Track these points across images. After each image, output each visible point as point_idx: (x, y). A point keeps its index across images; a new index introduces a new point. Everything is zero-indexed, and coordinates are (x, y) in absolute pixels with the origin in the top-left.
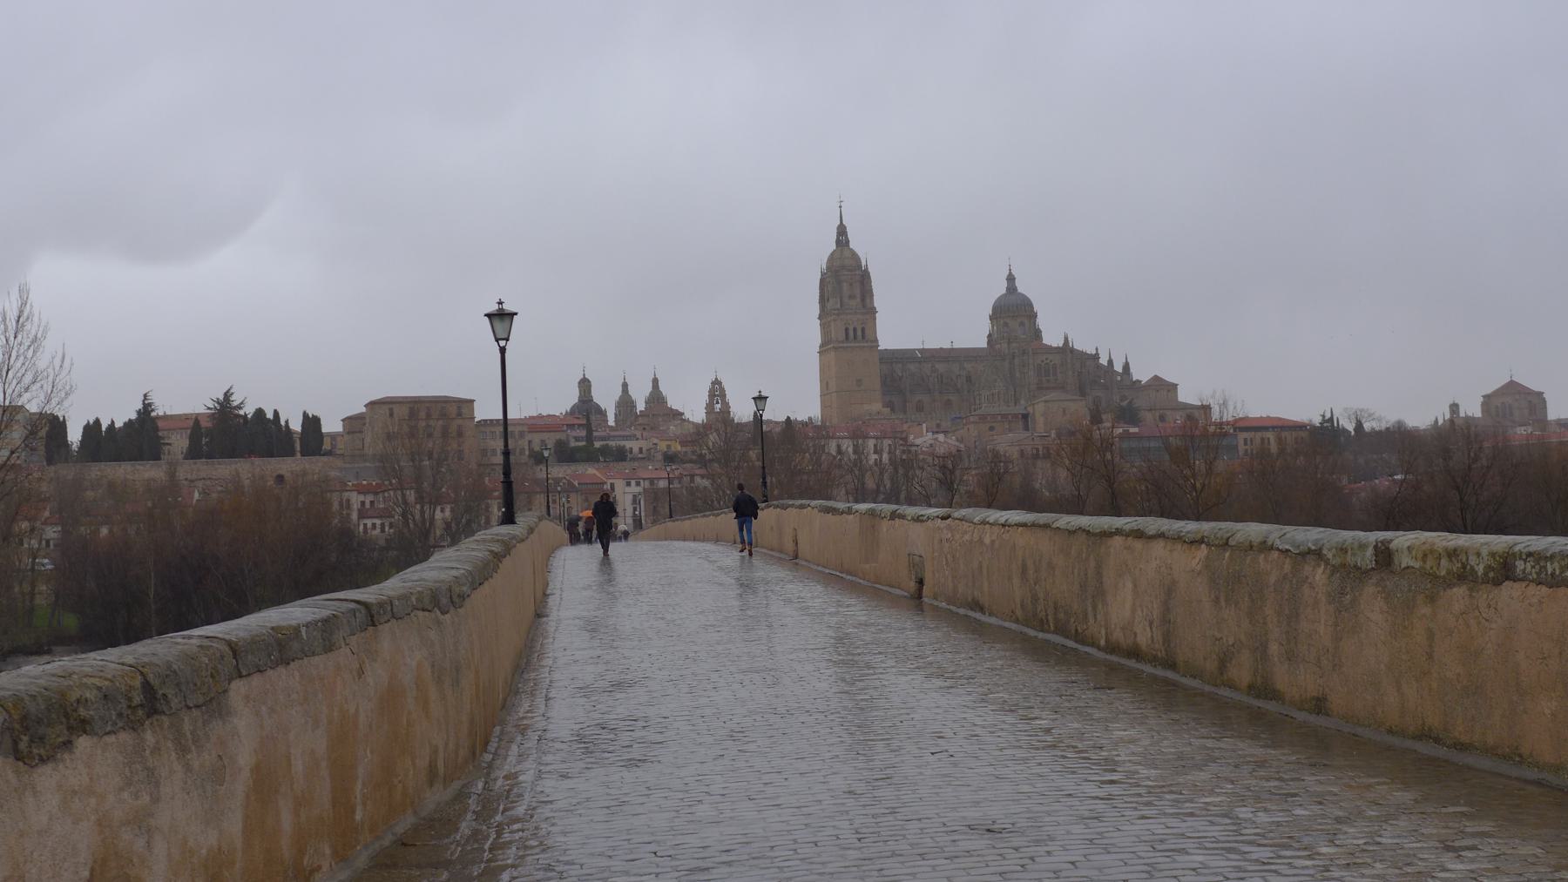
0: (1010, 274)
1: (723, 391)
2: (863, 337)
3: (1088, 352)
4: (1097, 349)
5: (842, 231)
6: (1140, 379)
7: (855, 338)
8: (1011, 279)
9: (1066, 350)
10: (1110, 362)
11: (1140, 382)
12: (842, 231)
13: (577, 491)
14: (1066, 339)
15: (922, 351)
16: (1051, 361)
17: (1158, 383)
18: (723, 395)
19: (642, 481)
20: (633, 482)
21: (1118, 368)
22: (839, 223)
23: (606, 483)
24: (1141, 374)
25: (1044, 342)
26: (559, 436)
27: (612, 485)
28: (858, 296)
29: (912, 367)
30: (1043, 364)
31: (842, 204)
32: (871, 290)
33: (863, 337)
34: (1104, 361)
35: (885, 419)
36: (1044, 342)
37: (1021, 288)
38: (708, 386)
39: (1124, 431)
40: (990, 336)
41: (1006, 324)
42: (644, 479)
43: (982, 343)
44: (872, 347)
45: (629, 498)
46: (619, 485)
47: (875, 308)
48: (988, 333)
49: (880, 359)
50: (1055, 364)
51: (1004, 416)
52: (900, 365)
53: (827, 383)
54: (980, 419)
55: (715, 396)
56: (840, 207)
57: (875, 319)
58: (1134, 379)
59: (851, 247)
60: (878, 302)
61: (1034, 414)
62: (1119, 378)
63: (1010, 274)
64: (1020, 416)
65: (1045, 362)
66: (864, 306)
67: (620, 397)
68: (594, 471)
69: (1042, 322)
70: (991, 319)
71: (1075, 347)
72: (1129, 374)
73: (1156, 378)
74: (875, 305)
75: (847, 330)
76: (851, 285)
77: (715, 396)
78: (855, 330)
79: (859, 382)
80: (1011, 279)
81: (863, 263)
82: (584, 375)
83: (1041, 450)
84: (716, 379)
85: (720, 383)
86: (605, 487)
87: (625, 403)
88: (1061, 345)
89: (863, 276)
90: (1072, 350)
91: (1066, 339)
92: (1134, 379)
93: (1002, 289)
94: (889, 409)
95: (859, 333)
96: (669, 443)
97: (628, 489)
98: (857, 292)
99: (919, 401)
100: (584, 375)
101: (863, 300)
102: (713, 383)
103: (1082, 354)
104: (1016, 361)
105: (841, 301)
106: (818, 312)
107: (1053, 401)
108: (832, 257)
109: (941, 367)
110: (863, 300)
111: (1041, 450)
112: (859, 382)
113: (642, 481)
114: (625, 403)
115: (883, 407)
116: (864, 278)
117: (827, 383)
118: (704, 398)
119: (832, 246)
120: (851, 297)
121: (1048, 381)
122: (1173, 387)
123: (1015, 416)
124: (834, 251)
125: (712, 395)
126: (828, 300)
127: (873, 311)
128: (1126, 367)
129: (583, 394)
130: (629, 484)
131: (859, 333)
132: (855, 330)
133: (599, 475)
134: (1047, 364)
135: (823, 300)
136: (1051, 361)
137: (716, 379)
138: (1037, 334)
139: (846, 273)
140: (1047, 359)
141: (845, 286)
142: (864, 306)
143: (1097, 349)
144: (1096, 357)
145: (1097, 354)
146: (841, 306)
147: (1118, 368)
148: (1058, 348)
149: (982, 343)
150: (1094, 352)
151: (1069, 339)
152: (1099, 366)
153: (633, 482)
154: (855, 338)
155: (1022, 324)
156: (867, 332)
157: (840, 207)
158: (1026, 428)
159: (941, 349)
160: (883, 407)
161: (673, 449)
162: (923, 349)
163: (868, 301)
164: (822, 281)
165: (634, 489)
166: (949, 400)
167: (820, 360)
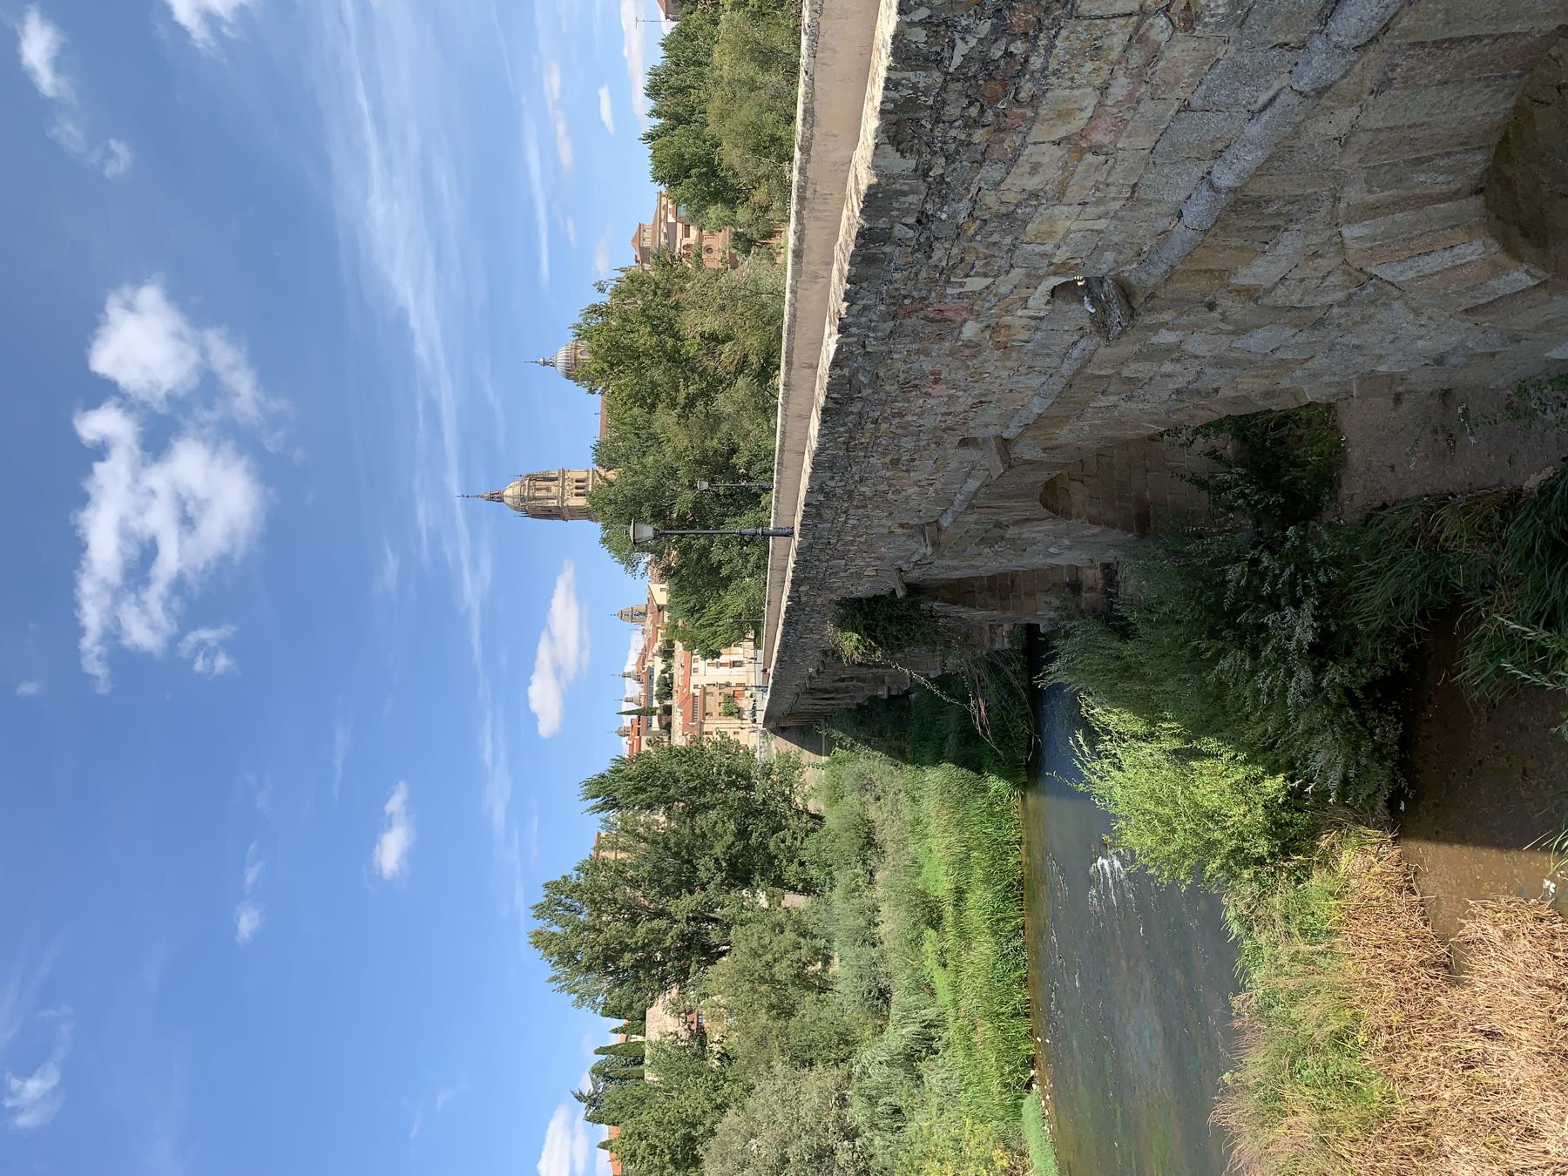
13: (702, 724)
27: (696, 687)
45: (712, 670)
66: (556, 479)
76: (537, 489)
78: (577, 488)
89: (530, 480)
97: (701, 672)
98: (544, 484)
128: (622, 270)
130: (696, 670)
132: (577, 488)
139: (526, 494)
142: (556, 479)
153: (694, 666)
154: (582, 488)
164: (533, 516)
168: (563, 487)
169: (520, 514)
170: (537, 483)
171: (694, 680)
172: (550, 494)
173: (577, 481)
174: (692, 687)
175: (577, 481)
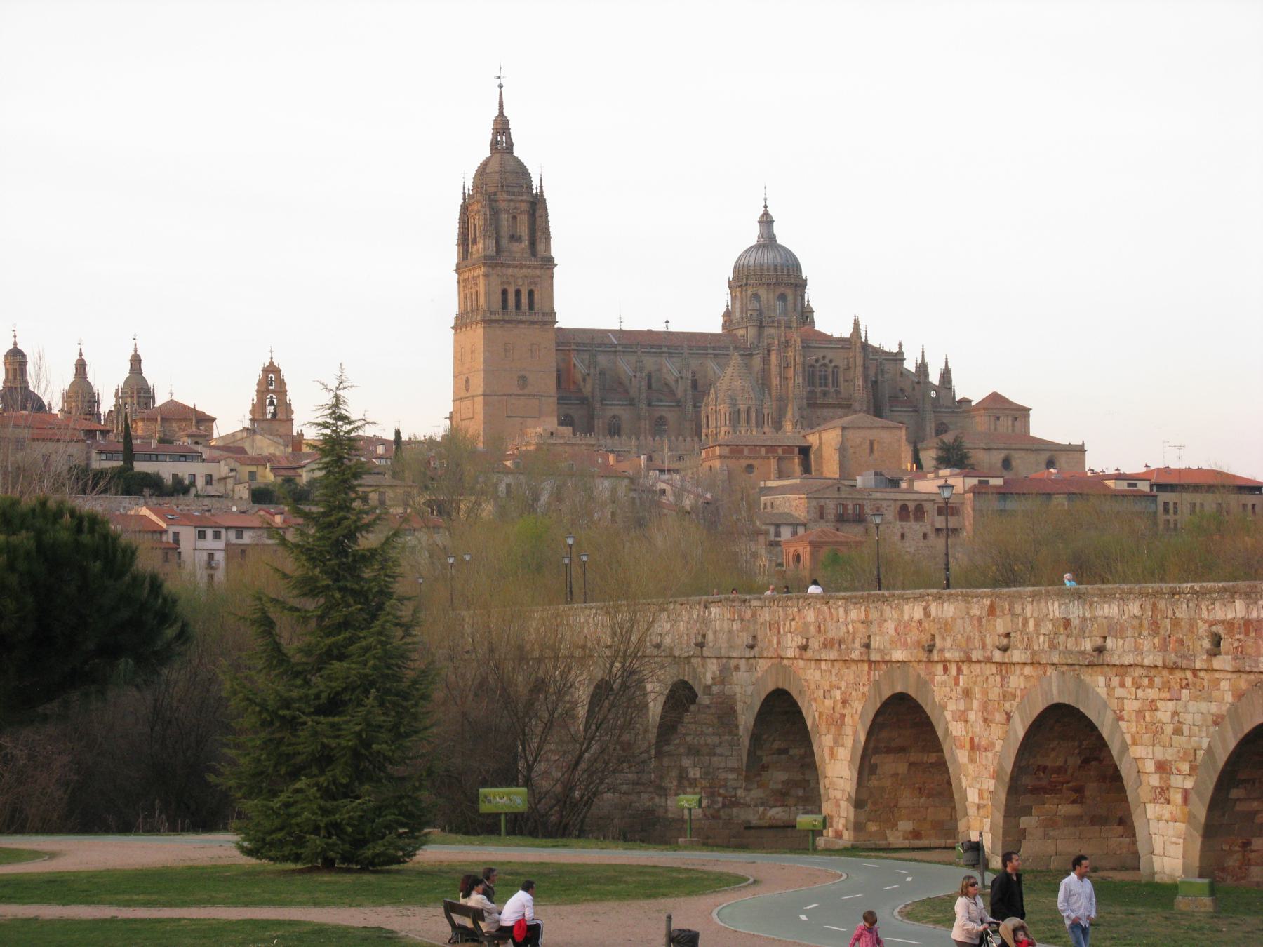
0: (766, 214)
1: (281, 383)
2: (531, 306)
3: (886, 349)
4: (900, 345)
5: (502, 127)
6: (970, 398)
7: (518, 305)
8: (766, 221)
9: (855, 344)
10: (923, 368)
11: (970, 401)
12: (502, 127)
14: (856, 325)
15: (621, 333)
16: (831, 361)
17: (996, 403)
18: (281, 390)
19: (223, 531)
20: (210, 533)
21: (934, 378)
22: (497, 113)
23: (166, 531)
24: (970, 388)
25: (816, 328)
26: (76, 450)
27: (176, 534)
28: (526, 238)
29: (603, 360)
30: (818, 365)
31: (503, 82)
32: (547, 229)
33: (531, 306)
34: (910, 365)
35: (565, 444)
36: (816, 328)
37: (783, 236)
38: (256, 374)
39: (980, 482)
40: (728, 315)
41: (756, 296)
42: (227, 528)
43: (715, 326)
44: (546, 323)
46: (187, 535)
47: (551, 260)
48: (724, 309)
49: (558, 344)
50: (836, 367)
51: (771, 449)
52: (586, 356)
53: (467, 381)
54: (731, 451)
55: (269, 391)
56: (501, 86)
57: (552, 277)
58: (958, 397)
59: (515, 154)
60: (559, 248)
61: (820, 449)
62: (933, 394)
63: (766, 214)
64: (797, 450)
65: (822, 362)
66: (534, 253)
67: (72, 385)
68: (145, 511)
69: (813, 295)
70: (730, 287)
71: (870, 342)
72: (950, 388)
73: (995, 398)
74: (553, 254)
75: (504, 292)
77: (269, 391)
78: (518, 293)
79: (523, 380)
80: (766, 221)
81: (535, 183)
82: (15, 344)
83: (850, 507)
84: (272, 363)
85: (277, 371)
86: (164, 538)
87: (82, 393)
88: (847, 335)
90: (865, 346)
91: (856, 325)
92: (958, 397)
93: (752, 236)
94: (570, 428)
95: (524, 299)
96: (253, 469)
97: (201, 544)
98: (523, 230)
99: (614, 417)
100: (15, 344)
101: (533, 243)
102: (266, 371)
103: (878, 351)
104: (774, 358)
105: (497, 243)
106: (456, 261)
107: (854, 428)
108: (482, 171)
109: (650, 363)
110: (533, 243)
111: (850, 507)
112: (523, 380)
113: (223, 531)
114: (82, 393)
115: (561, 423)
116: (536, 206)
117: (467, 381)
118: (250, 394)
119: (484, 152)
120: (514, 238)
121: (825, 394)
122: (1021, 413)
123: (789, 449)
124: (488, 160)
125: (263, 389)
126: (475, 242)
127: (549, 263)
128: (946, 376)
129: (11, 377)
130: (202, 535)
131: (524, 299)
132: (518, 293)
133: (154, 518)
134: (825, 365)
135: (464, 240)
136: (831, 361)
137: (272, 363)
138: (806, 315)
140: (824, 358)
141: (504, 216)
143: (900, 345)
144: (898, 357)
145: (900, 353)
146: (498, 251)
147: (934, 378)
148: (842, 340)
149: (715, 326)
150: (895, 350)
151: (862, 327)
152: (904, 373)
153: (210, 533)
154: (518, 305)
155: (782, 297)
156: (537, 297)
157: (501, 86)
158: (806, 469)
159: (650, 332)
160: (561, 423)
161: (259, 479)
162: (621, 331)
163: (540, 247)
164: (465, 209)
165: (210, 543)
166: (661, 418)
167: (456, 341)
168: (522, 266)
169: (469, 184)
170: (524, 220)
171: (187, 535)
172: (505, 242)
173: (531, 293)
174: (176, 529)
175: (531, 293)
